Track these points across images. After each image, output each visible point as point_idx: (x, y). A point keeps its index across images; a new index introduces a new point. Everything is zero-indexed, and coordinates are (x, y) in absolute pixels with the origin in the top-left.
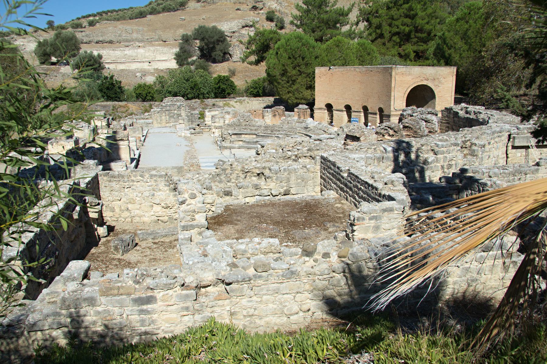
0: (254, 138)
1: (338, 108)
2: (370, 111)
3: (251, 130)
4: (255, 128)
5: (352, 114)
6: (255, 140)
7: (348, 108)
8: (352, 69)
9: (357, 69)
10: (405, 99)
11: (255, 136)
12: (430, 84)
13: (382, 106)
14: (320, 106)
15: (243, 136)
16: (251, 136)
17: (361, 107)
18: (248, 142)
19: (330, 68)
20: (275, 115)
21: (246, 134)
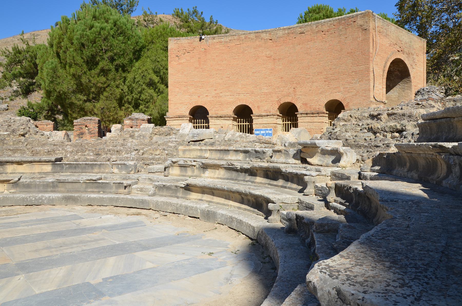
0: (47, 174)
1: (220, 113)
2: (300, 111)
3: (34, 153)
4: (47, 148)
5: (254, 122)
6: (50, 179)
7: (244, 114)
8: (252, 36)
9: (263, 35)
10: (385, 80)
11: (48, 168)
12: (406, 62)
13: (338, 97)
14: (178, 113)
15: (10, 168)
16: (37, 168)
17: (277, 106)
18: (28, 186)
19: (201, 39)
20: (82, 134)
21: (19, 163)
